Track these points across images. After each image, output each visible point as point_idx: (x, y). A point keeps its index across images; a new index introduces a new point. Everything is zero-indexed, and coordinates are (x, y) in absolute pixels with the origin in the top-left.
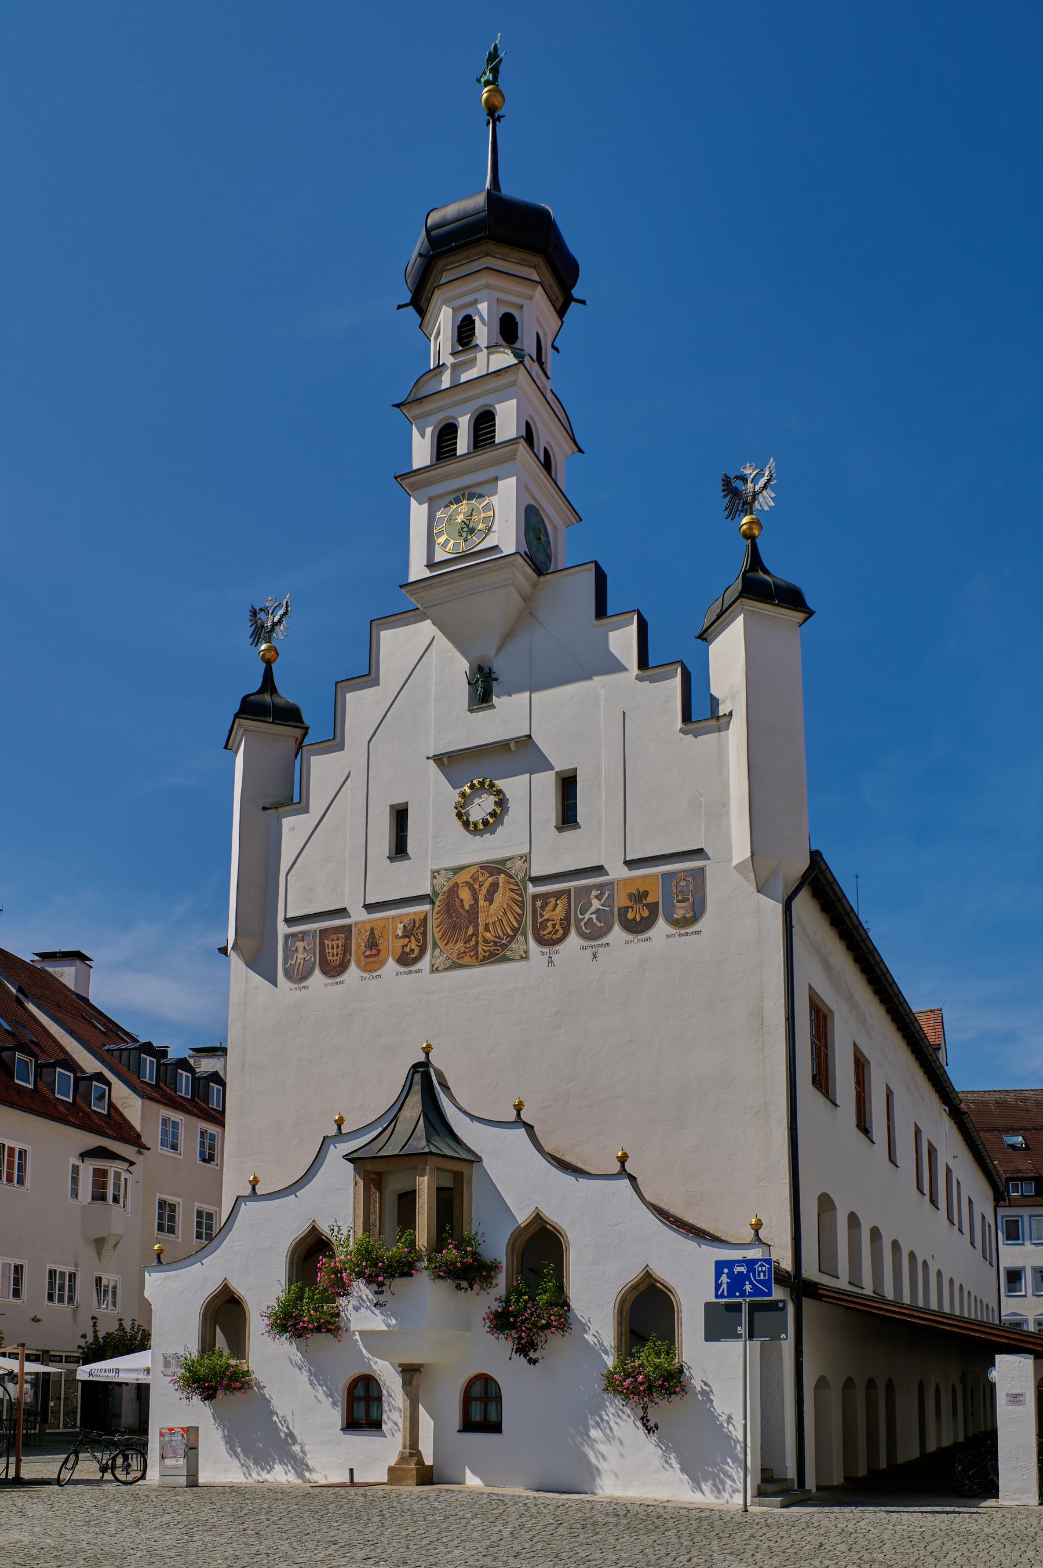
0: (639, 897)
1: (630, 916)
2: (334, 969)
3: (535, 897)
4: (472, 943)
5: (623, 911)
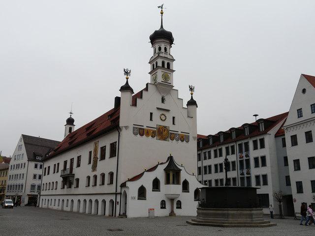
2: (142, 135)
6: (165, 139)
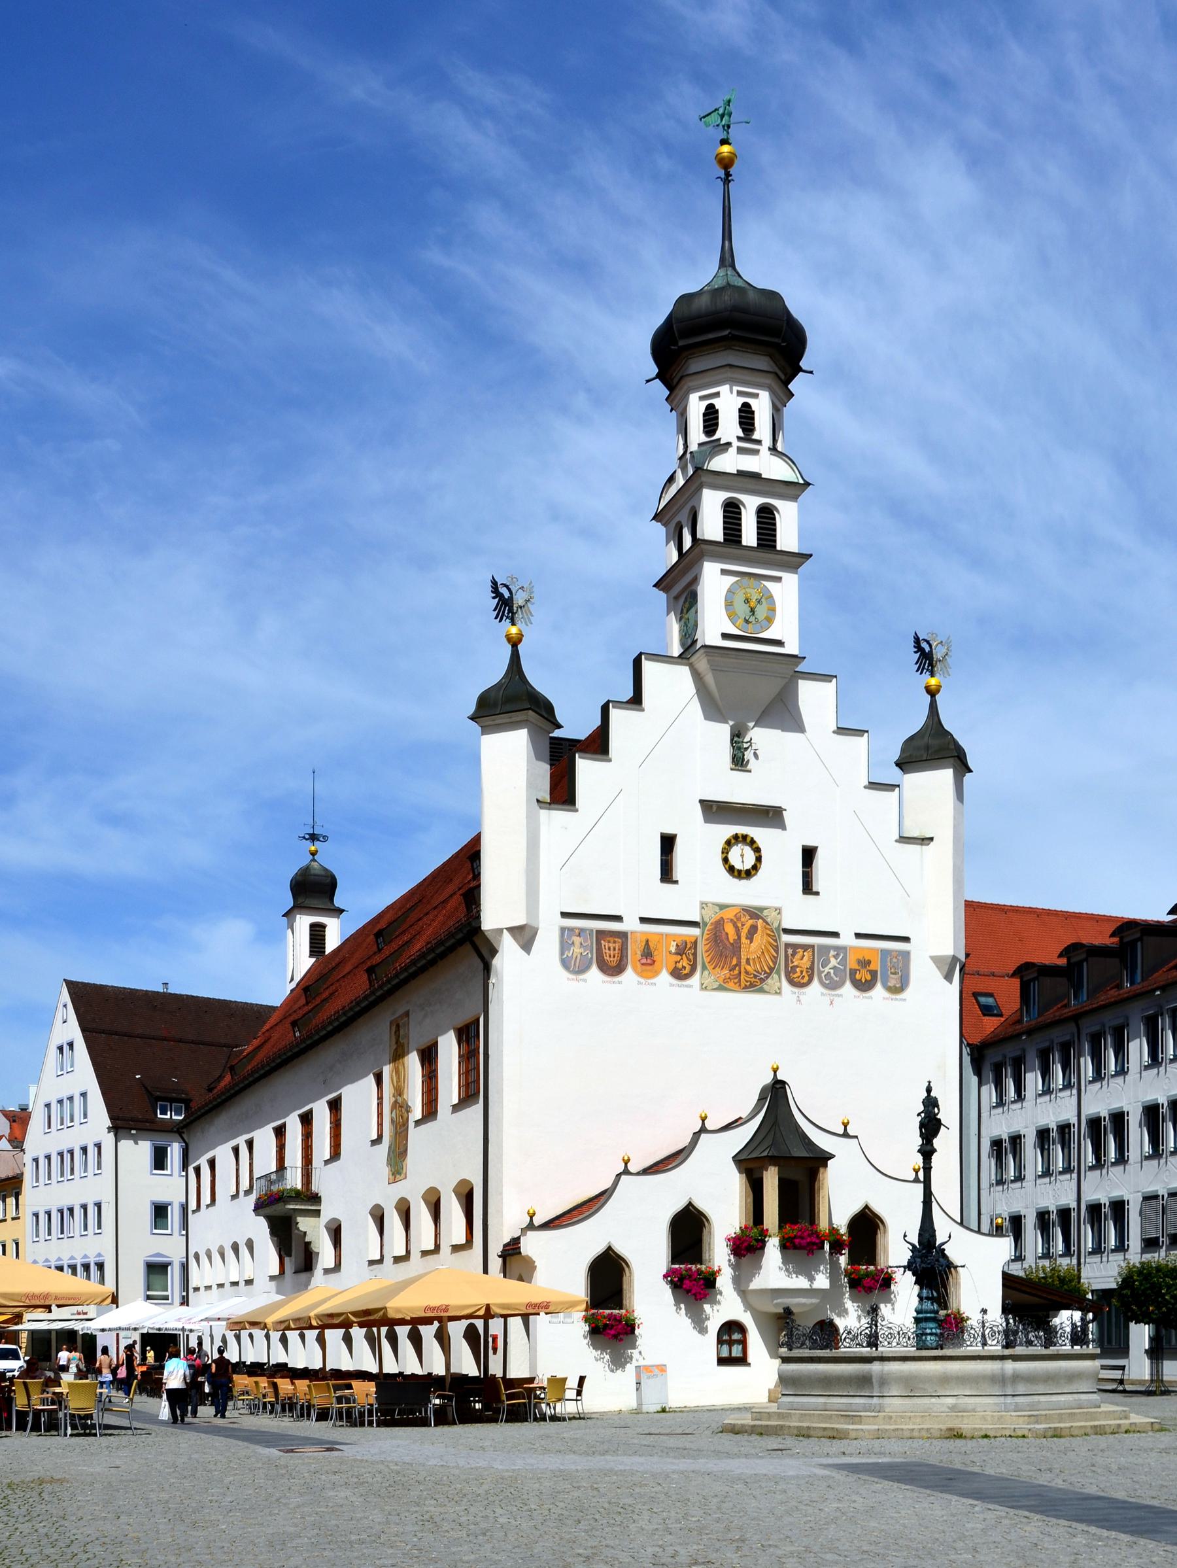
0: (865, 963)
1: (858, 977)
2: (613, 969)
3: (787, 945)
4: (736, 972)
5: (853, 973)
6: (755, 984)
